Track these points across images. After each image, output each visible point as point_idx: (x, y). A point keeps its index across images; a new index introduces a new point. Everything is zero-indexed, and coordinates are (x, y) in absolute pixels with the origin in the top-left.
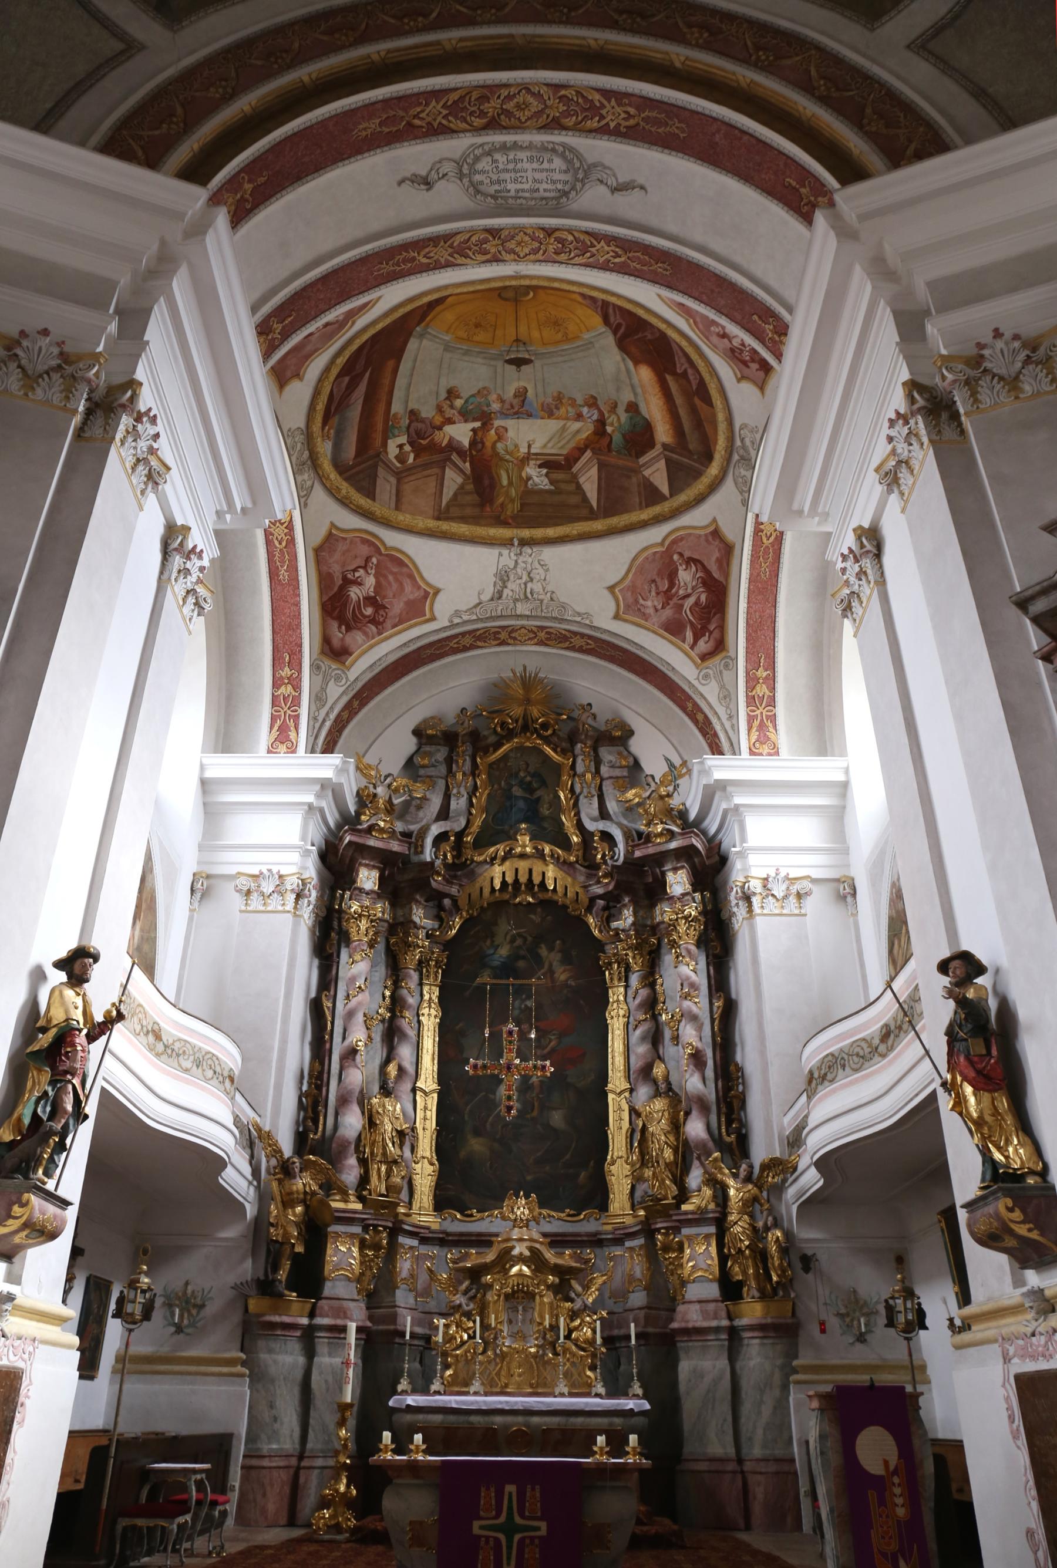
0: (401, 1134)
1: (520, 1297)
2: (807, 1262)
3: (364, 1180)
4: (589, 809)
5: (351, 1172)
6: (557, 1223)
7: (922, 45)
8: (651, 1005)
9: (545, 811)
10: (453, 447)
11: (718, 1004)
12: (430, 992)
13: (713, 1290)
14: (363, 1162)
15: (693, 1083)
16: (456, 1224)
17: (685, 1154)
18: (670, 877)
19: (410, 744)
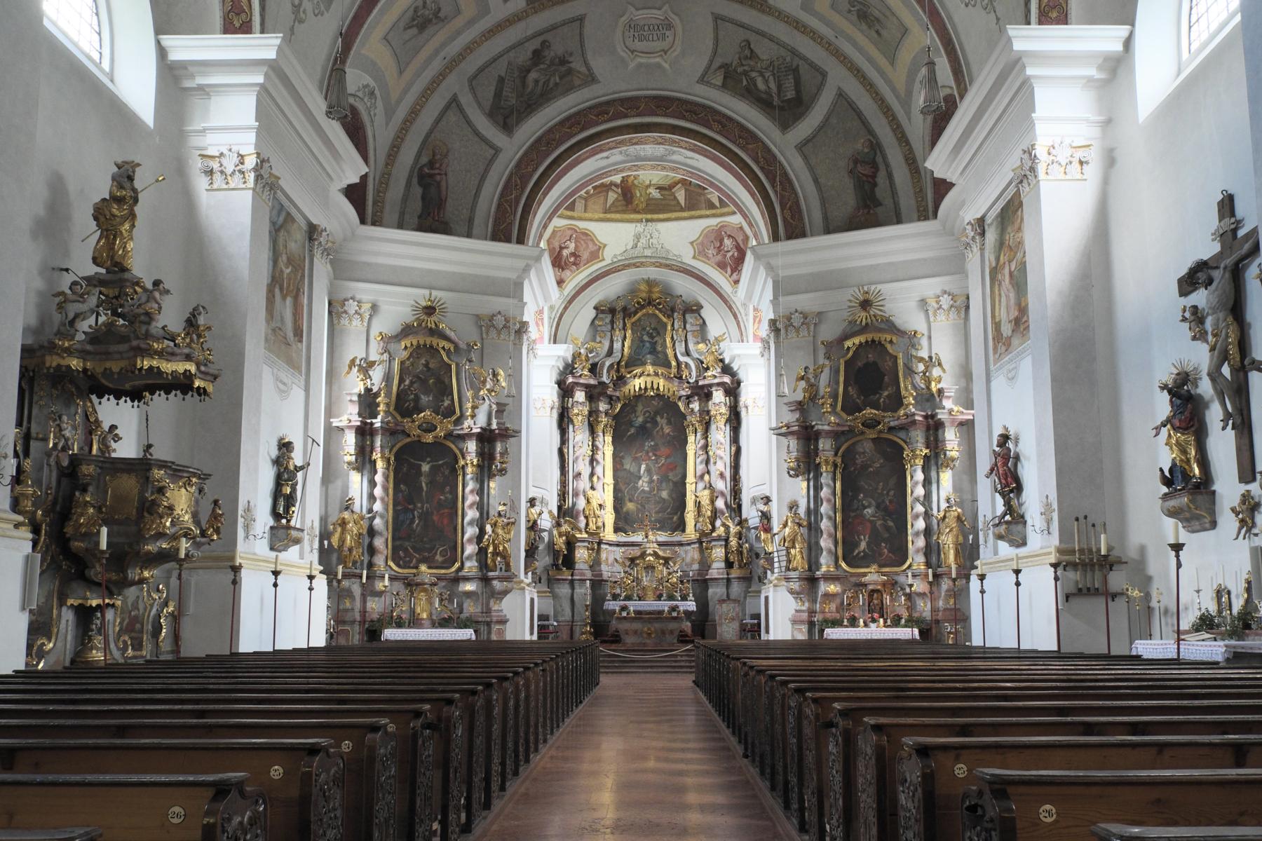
0: (600, 505)
1: (650, 568)
2: (757, 556)
3: (587, 524)
4: (680, 348)
5: (582, 523)
6: (663, 537)
7: (801, 147)
8: (706, 447)
9: (659, 348)
10: (612, 184)
11: (734, 449)
12: (609, 439)
13: (723, 565)
14: (586, 517)
15: (720, 485)
16: (622, 538)
17: (715, 514)
18: (715, 394)
19: (593, 313)
